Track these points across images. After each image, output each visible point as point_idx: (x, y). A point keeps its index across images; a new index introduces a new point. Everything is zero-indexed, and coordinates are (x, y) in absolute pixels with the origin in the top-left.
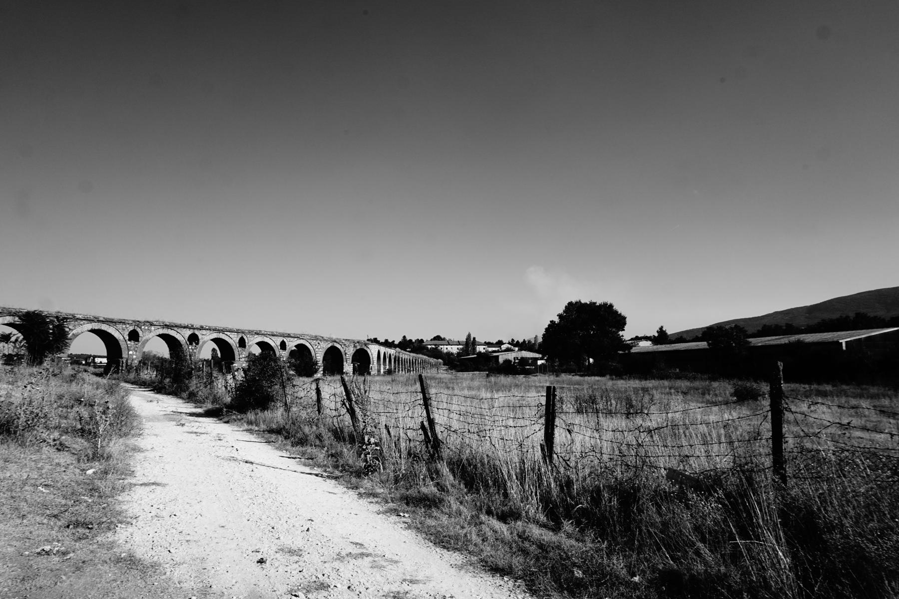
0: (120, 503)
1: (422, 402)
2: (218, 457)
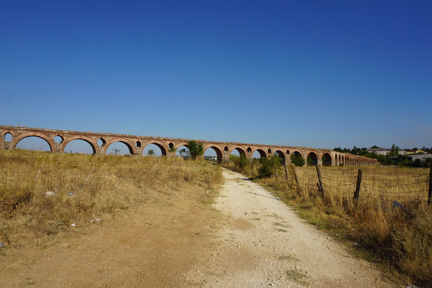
0: (214, 199)
2: (246, 192)
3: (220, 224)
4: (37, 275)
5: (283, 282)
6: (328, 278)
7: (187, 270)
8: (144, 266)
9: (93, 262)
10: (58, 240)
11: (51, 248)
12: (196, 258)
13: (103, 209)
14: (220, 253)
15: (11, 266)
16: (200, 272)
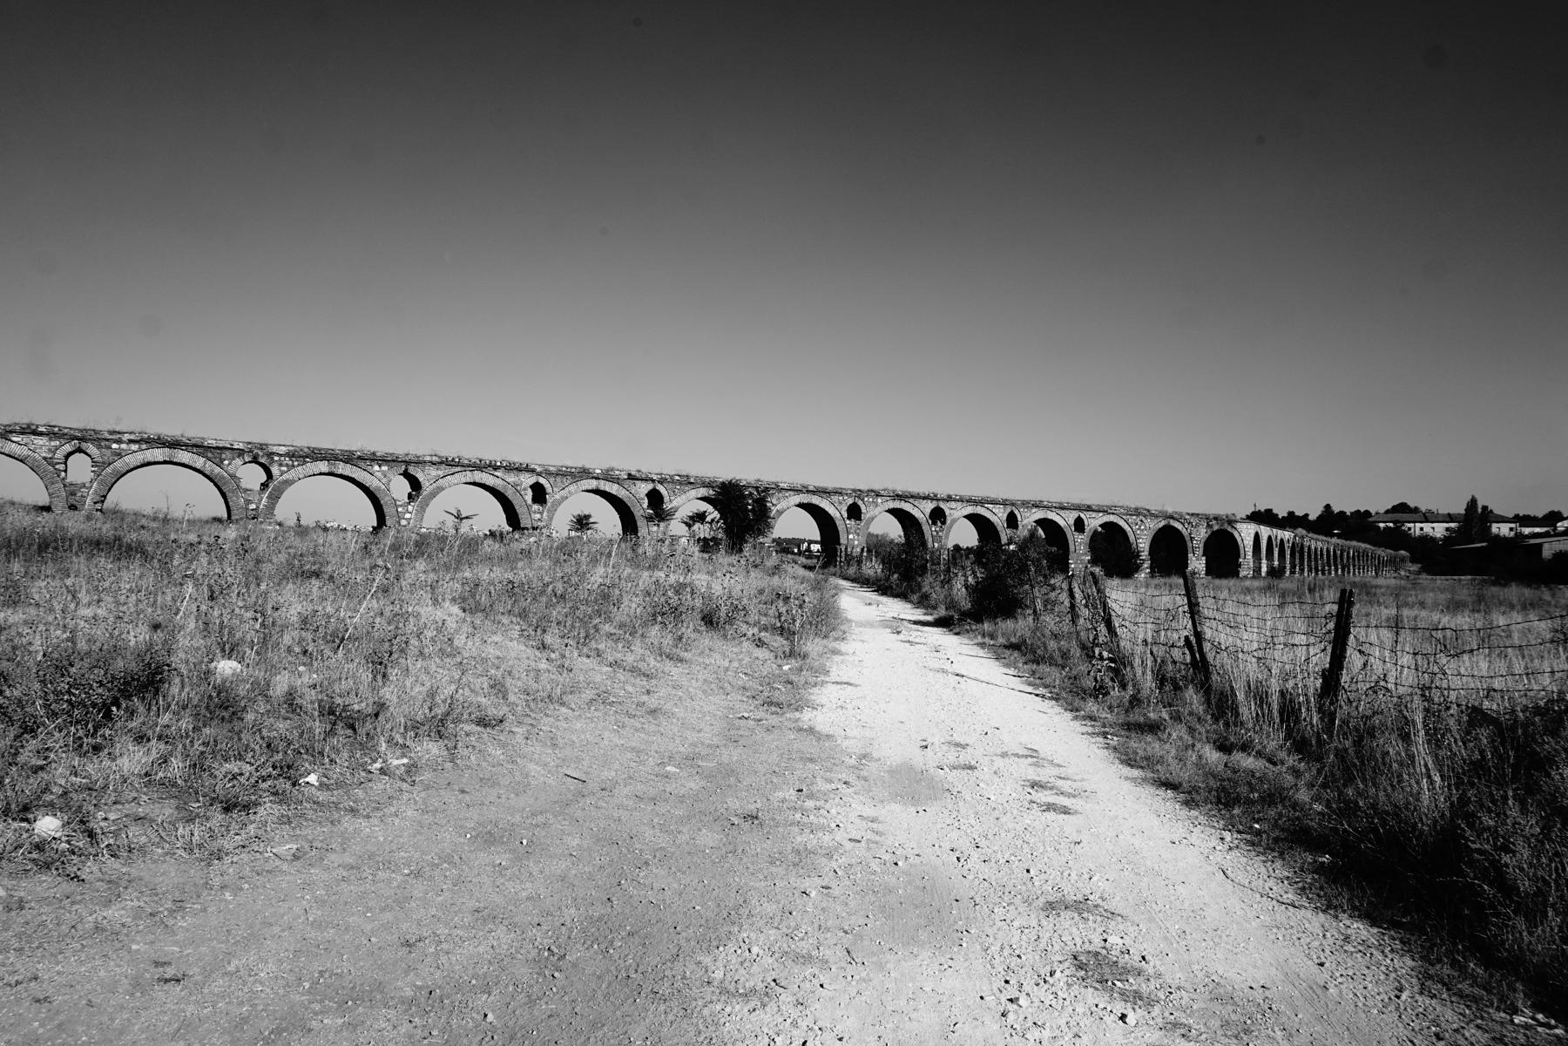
1: (1186, 608)
3: (831, 781)
4: (189, 951)
5: (1060, 993)
6: (1222, 982)
7: (715, 943)
8: (563, 928)
9: (382, 910)
10: (260, 832)
11: (235, 860)
12: (745, 901)
13: (415, 727)
14: (833, 884)
15: (100, 919)
16: (761, 952)
